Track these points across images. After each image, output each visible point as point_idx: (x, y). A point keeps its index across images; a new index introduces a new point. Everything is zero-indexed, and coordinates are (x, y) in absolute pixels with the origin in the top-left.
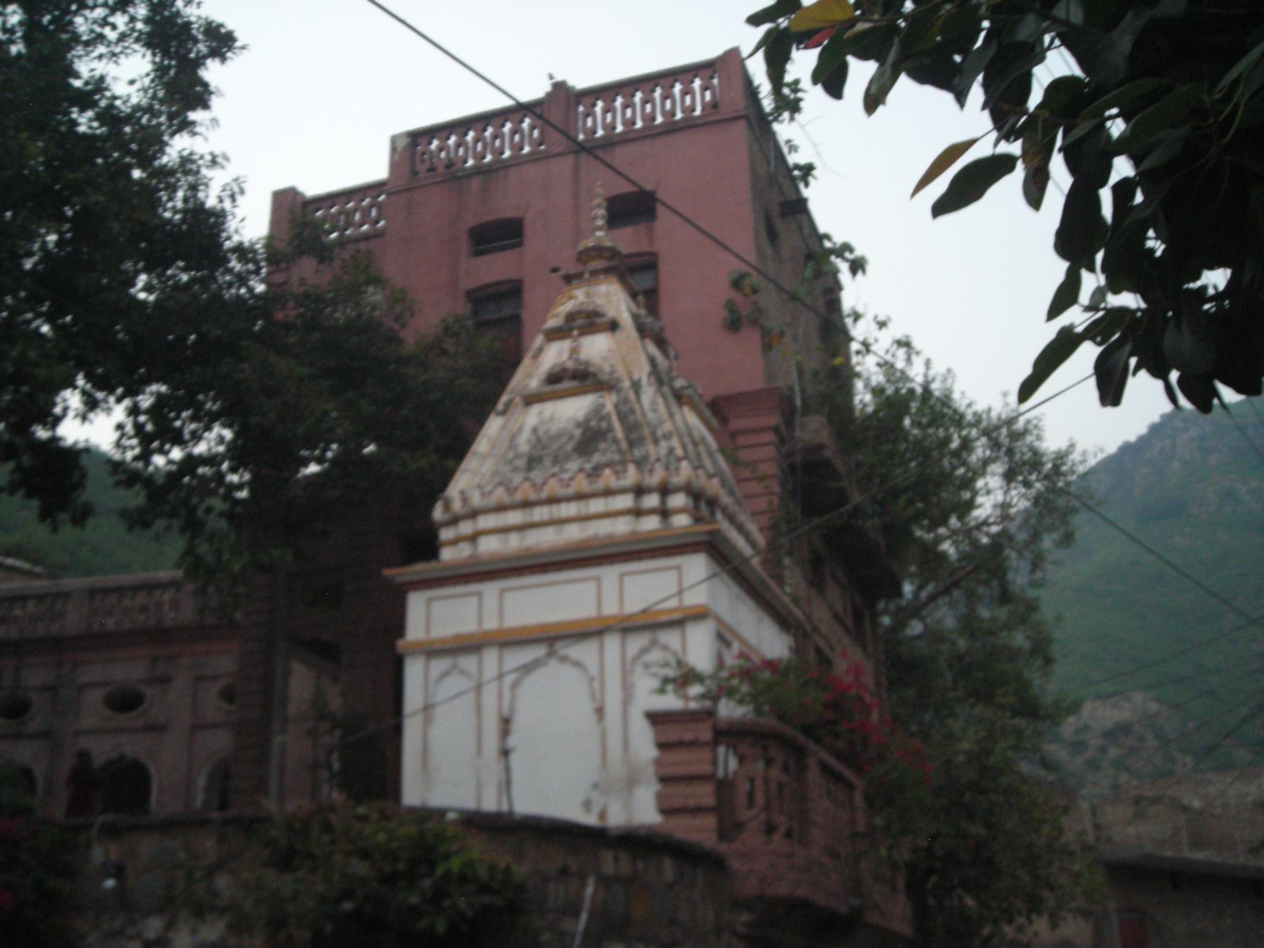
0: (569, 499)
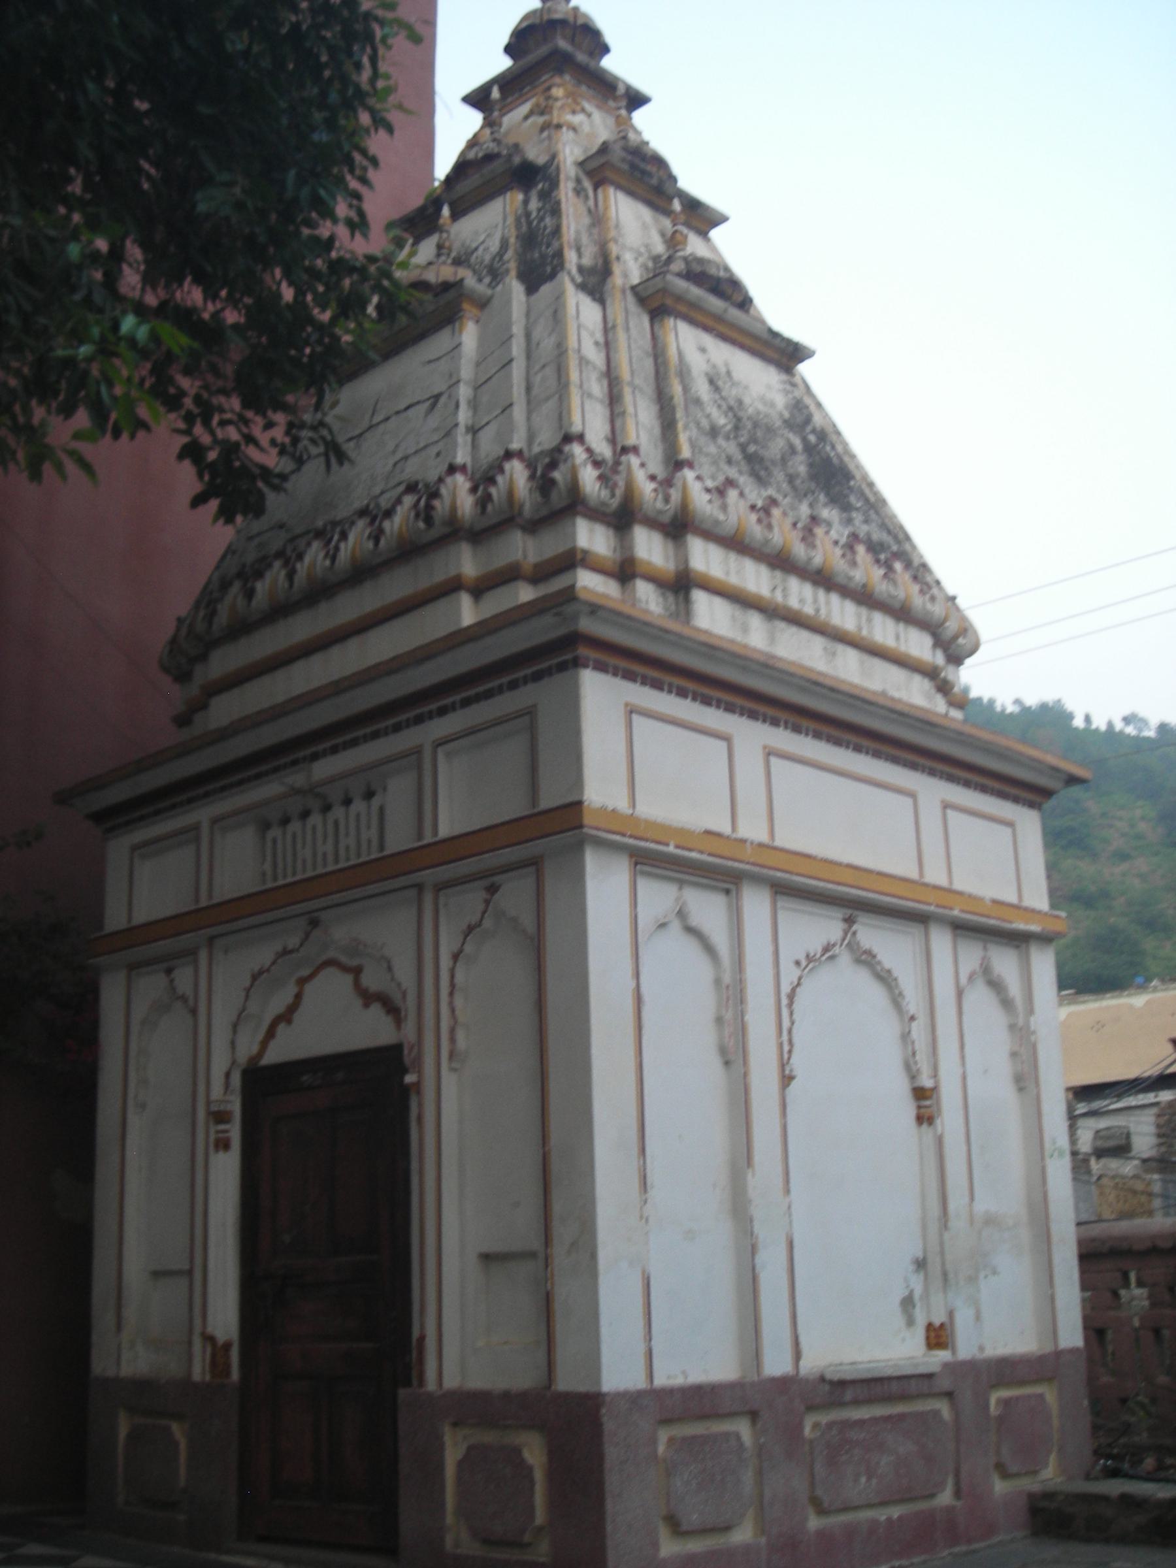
0: (847, 592)
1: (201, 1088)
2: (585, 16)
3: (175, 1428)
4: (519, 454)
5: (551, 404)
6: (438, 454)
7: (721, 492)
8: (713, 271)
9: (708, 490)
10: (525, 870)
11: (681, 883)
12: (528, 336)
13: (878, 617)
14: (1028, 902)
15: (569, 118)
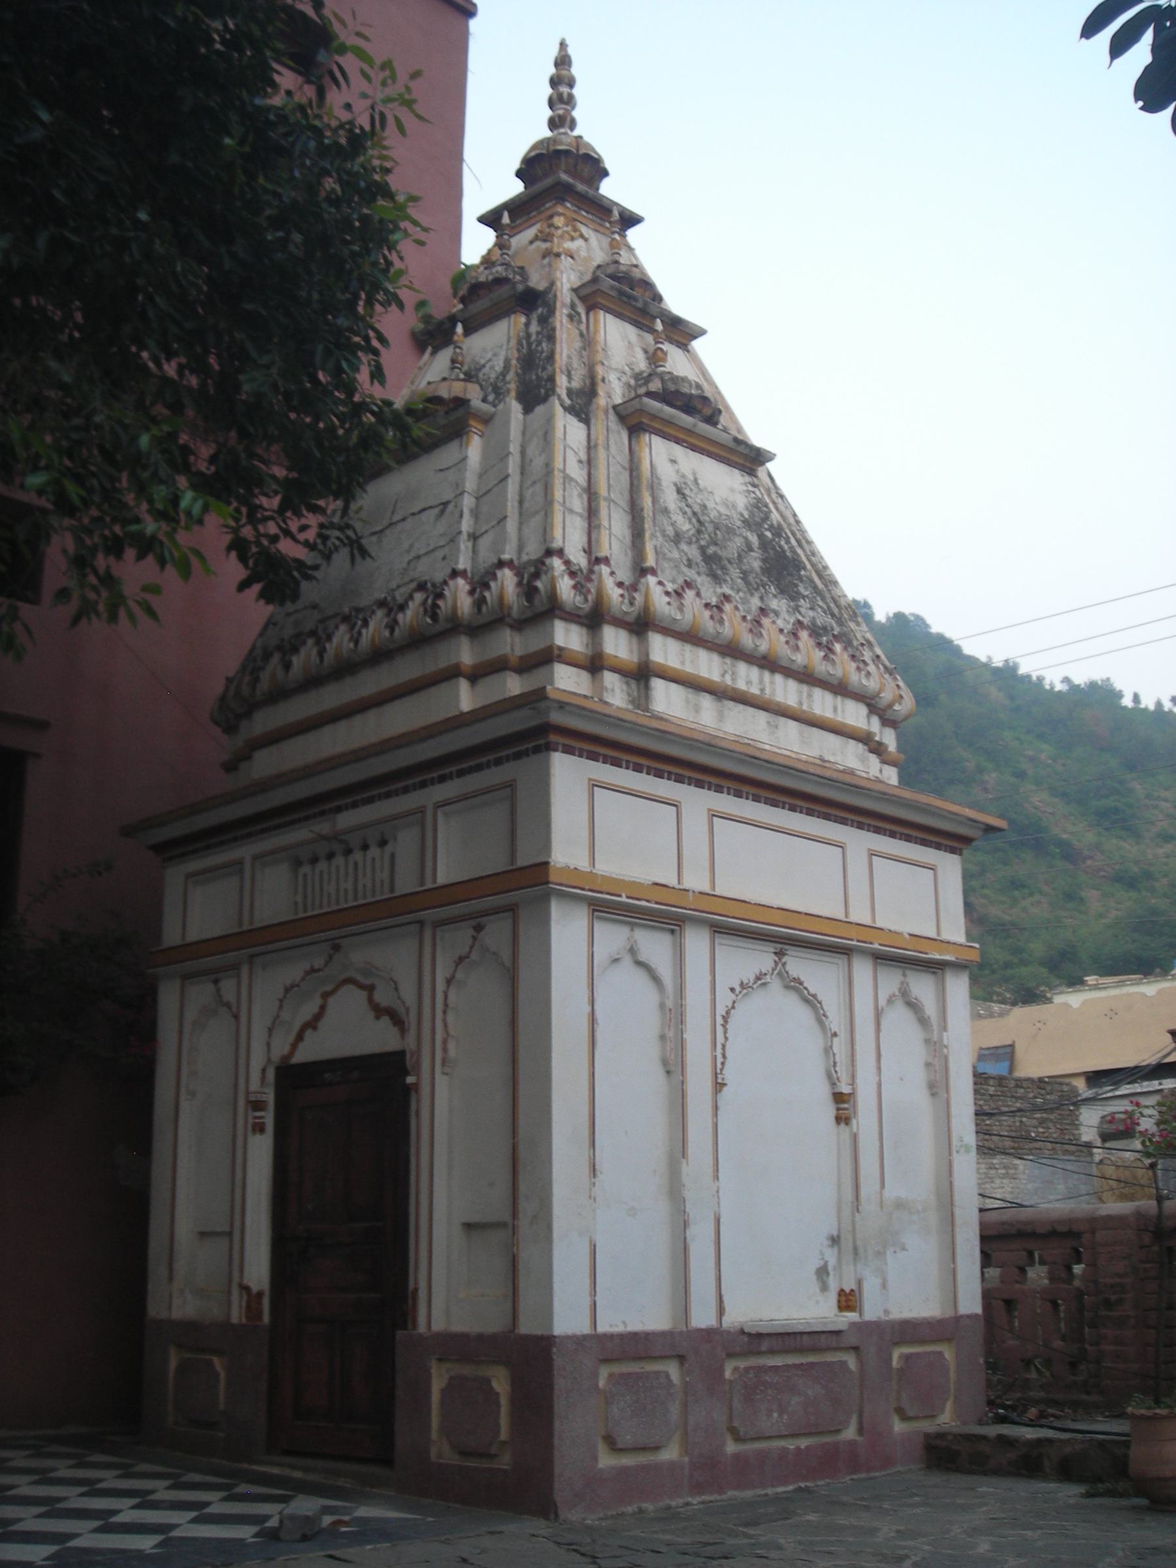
0: (789, 672)
1: (242, 1081)
2: (588, 145)
3: (216, 1361)
4: (510, 564)
5: (539, 518)
6: (444, 558)
7: (678, 594)
8: (685, 390)
9: (667, 593)
10: (502, 915)
11: (633, 926)
12: (523, 453)
13: (818, 693)
14: (945, 936)
15: (568, 245)
